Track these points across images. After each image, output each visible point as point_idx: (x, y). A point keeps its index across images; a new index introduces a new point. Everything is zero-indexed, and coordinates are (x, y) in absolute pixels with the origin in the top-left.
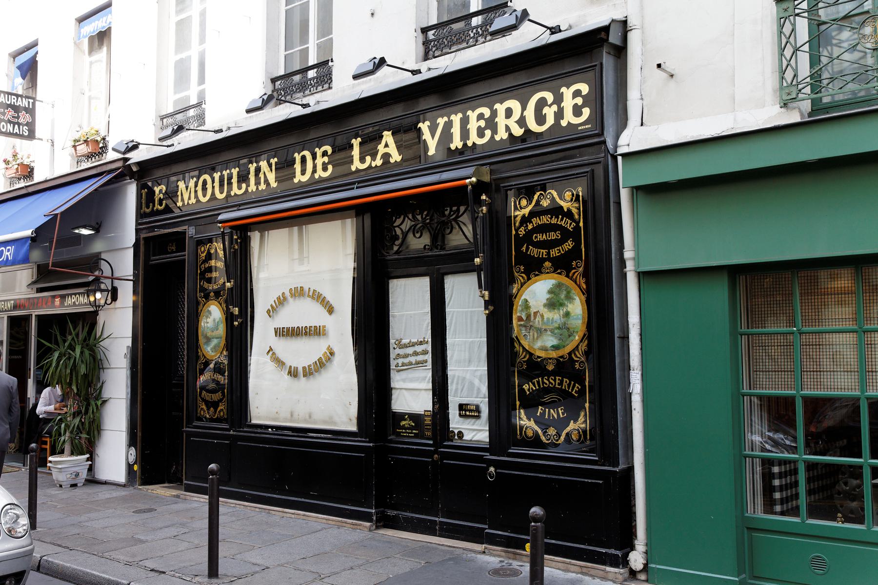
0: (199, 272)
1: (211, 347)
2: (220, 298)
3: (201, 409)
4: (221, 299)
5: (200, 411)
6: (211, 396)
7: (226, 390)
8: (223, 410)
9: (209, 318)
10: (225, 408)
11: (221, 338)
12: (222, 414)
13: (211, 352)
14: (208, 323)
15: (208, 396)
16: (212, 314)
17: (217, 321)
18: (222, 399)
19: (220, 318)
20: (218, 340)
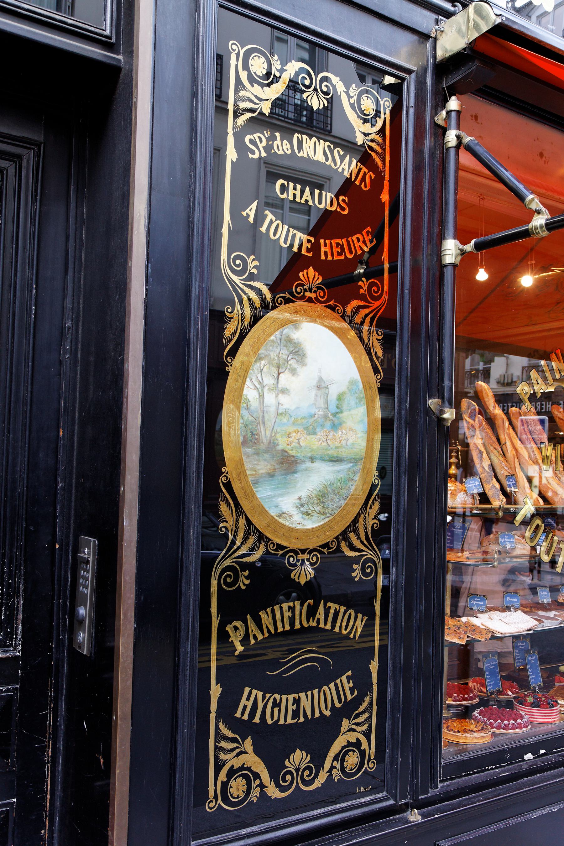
0: (231, 154)
1: (304, 494)
2: (356, 303)
3: (232, 772)
4: (360, 307)
5: (225, 785)
6: (297, 702)
7: (374, 666)
8: (358, 744)
9: (293, 372)
10: (367, 734)
11: (355, 461)
12: (352, 760)
13: (297, 517)
14: (284, 391)
15: (276, 704)
16: (308, 360)
17: (334, 392)
18: (358, 701)
19: (352, 383)
20: (338, 467)
